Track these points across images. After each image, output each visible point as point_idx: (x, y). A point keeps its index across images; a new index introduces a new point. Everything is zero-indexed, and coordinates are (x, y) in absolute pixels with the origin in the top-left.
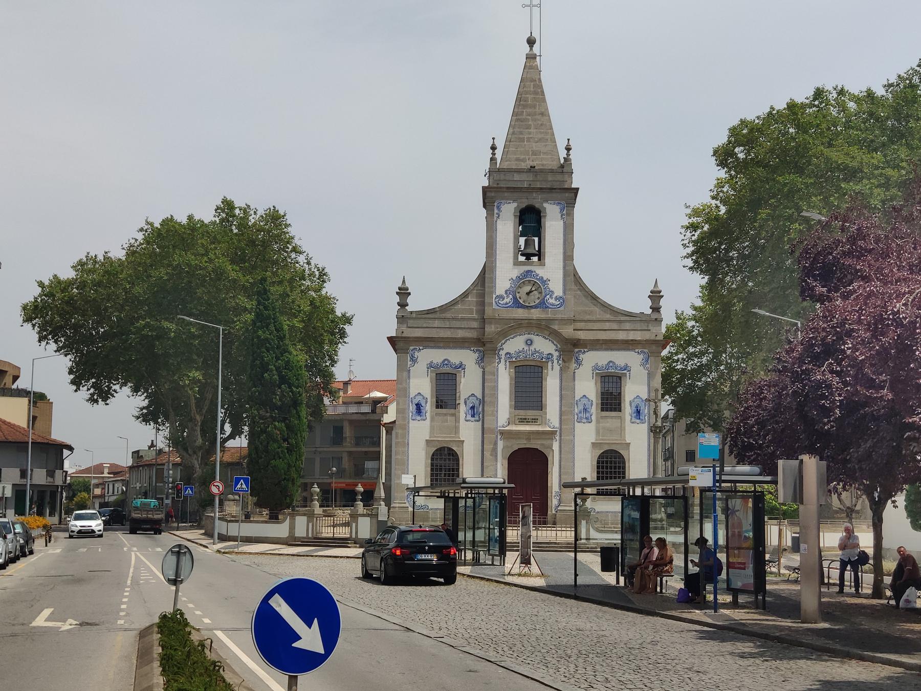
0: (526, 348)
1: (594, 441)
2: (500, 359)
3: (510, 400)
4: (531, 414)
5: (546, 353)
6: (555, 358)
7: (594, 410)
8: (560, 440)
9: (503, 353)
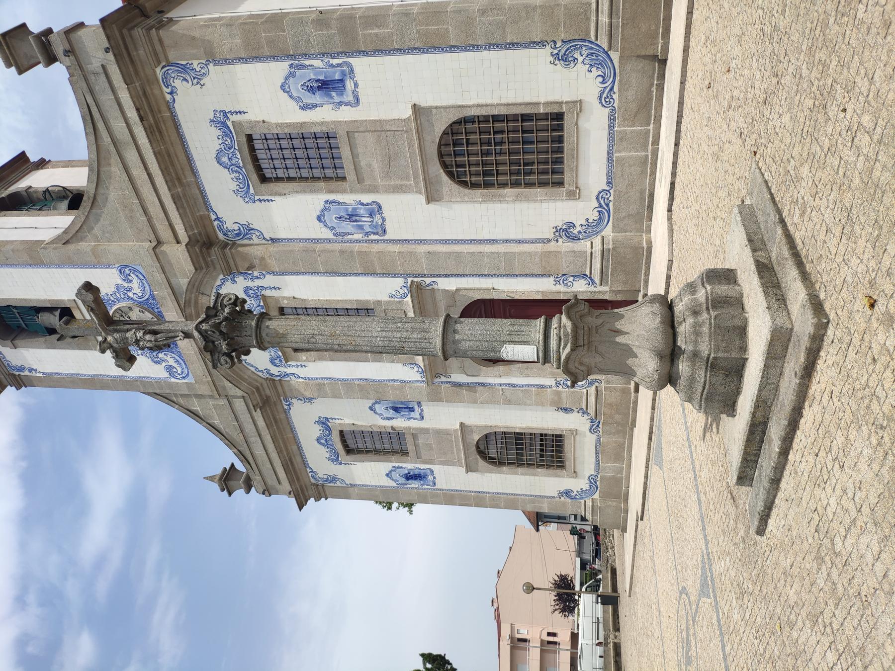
1: (422, 198)
6: (250, 284)
7: (349, 199)
8: (431, 275)
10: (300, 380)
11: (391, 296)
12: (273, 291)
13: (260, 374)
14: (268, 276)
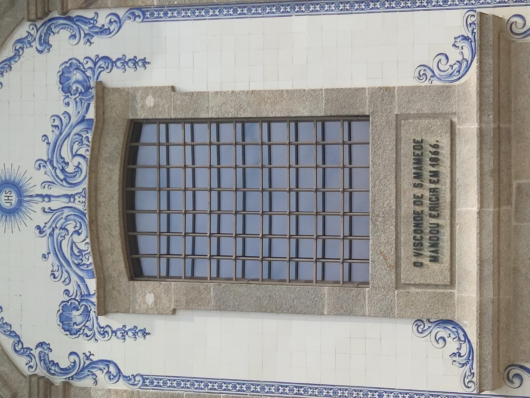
0: (36, 215)
2: (89, 366)
3: (313, 310)
4: (385, 187)
5: (55, 103)
6: (82, 51)
9: (63, 349)
10: (122, 385)
11: (424, 71)
12: (130, 71)
13: (21, 361)
14: (129, 25)
